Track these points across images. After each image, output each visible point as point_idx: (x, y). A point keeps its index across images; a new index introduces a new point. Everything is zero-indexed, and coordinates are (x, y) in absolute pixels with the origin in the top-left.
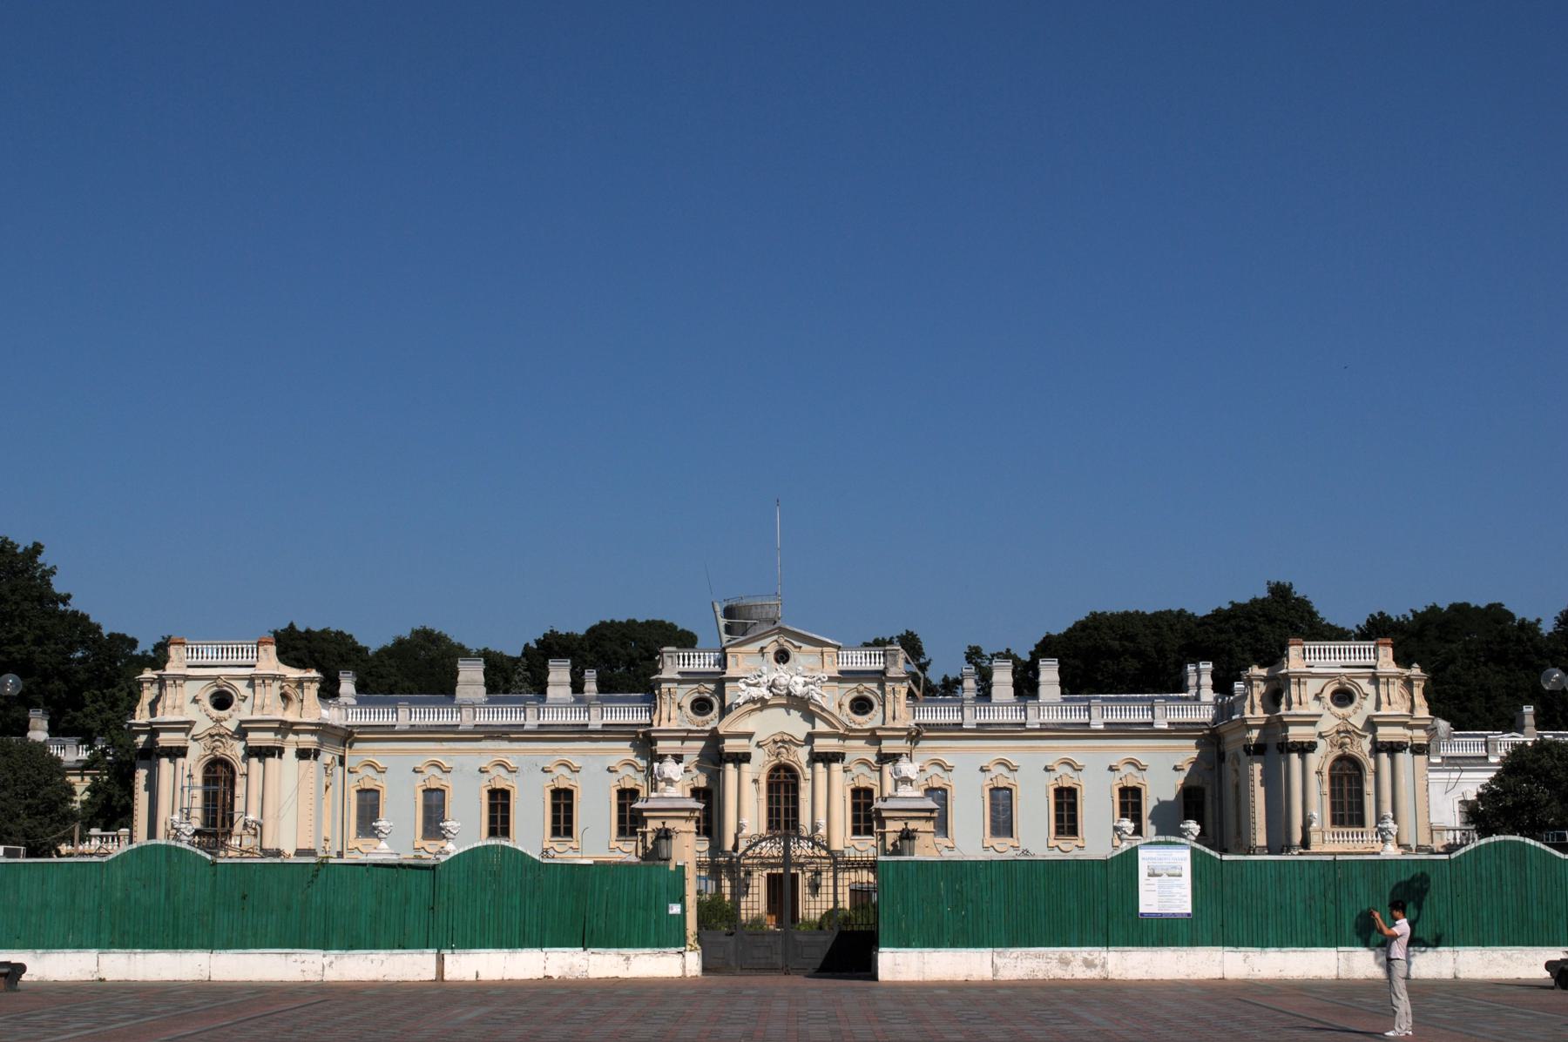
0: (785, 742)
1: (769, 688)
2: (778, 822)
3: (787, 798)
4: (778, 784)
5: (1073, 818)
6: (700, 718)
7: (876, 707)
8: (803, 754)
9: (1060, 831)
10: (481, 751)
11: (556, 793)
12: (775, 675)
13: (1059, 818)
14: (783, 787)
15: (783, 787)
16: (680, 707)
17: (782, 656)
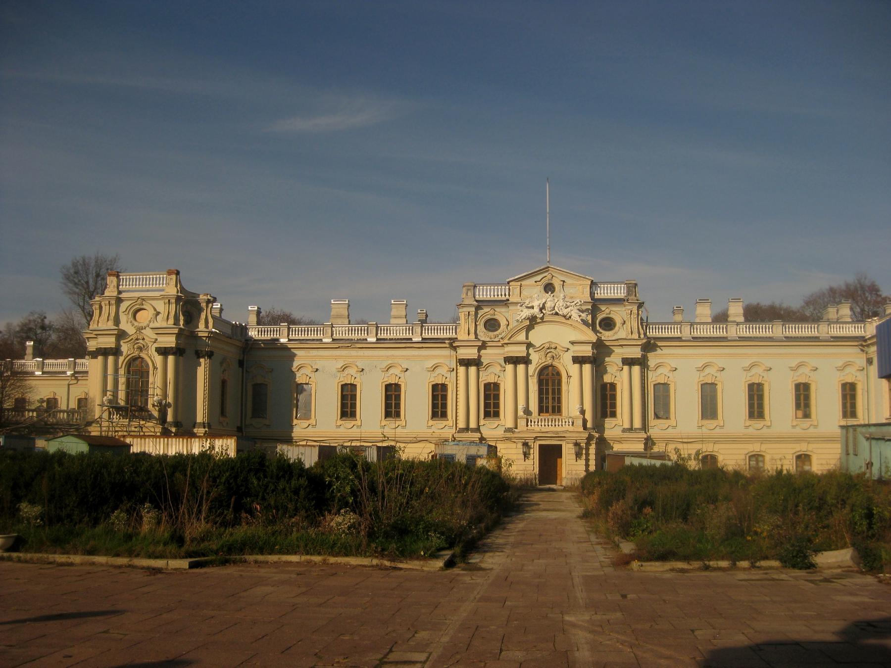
0: (549, 349)
1: (541, 310)
2: (547, 408)
3: (553, 390)
4: (547, 381)
5: (761, 406)
6: (492, 334)
7: (618, 324)
8: (567, 358)
9: (751, 415)
10: (336, 358)
11: (388, 387)
12: (544, 301)
13: (751, 406)
14: (549, 385)
15: (549, 385)
16: (476, 325)
17: (549, 288)
